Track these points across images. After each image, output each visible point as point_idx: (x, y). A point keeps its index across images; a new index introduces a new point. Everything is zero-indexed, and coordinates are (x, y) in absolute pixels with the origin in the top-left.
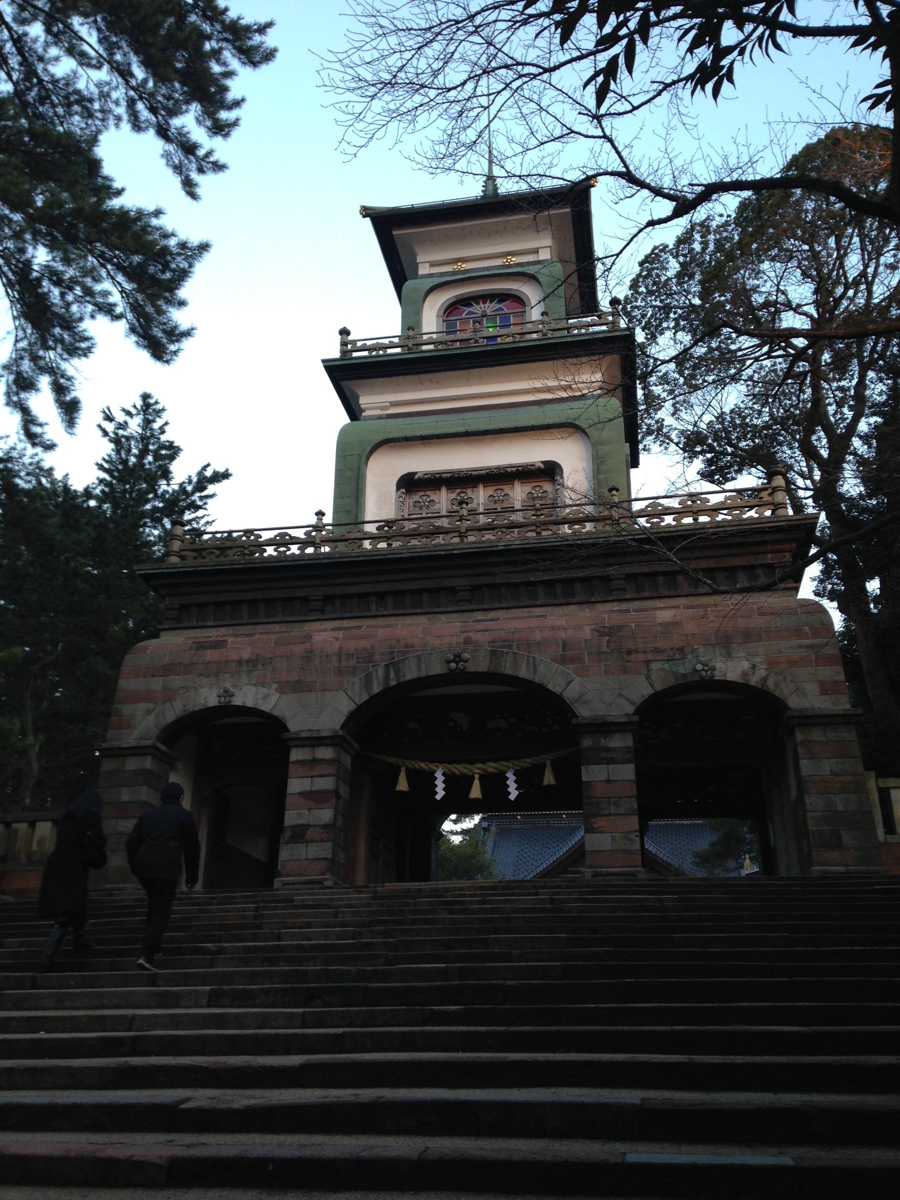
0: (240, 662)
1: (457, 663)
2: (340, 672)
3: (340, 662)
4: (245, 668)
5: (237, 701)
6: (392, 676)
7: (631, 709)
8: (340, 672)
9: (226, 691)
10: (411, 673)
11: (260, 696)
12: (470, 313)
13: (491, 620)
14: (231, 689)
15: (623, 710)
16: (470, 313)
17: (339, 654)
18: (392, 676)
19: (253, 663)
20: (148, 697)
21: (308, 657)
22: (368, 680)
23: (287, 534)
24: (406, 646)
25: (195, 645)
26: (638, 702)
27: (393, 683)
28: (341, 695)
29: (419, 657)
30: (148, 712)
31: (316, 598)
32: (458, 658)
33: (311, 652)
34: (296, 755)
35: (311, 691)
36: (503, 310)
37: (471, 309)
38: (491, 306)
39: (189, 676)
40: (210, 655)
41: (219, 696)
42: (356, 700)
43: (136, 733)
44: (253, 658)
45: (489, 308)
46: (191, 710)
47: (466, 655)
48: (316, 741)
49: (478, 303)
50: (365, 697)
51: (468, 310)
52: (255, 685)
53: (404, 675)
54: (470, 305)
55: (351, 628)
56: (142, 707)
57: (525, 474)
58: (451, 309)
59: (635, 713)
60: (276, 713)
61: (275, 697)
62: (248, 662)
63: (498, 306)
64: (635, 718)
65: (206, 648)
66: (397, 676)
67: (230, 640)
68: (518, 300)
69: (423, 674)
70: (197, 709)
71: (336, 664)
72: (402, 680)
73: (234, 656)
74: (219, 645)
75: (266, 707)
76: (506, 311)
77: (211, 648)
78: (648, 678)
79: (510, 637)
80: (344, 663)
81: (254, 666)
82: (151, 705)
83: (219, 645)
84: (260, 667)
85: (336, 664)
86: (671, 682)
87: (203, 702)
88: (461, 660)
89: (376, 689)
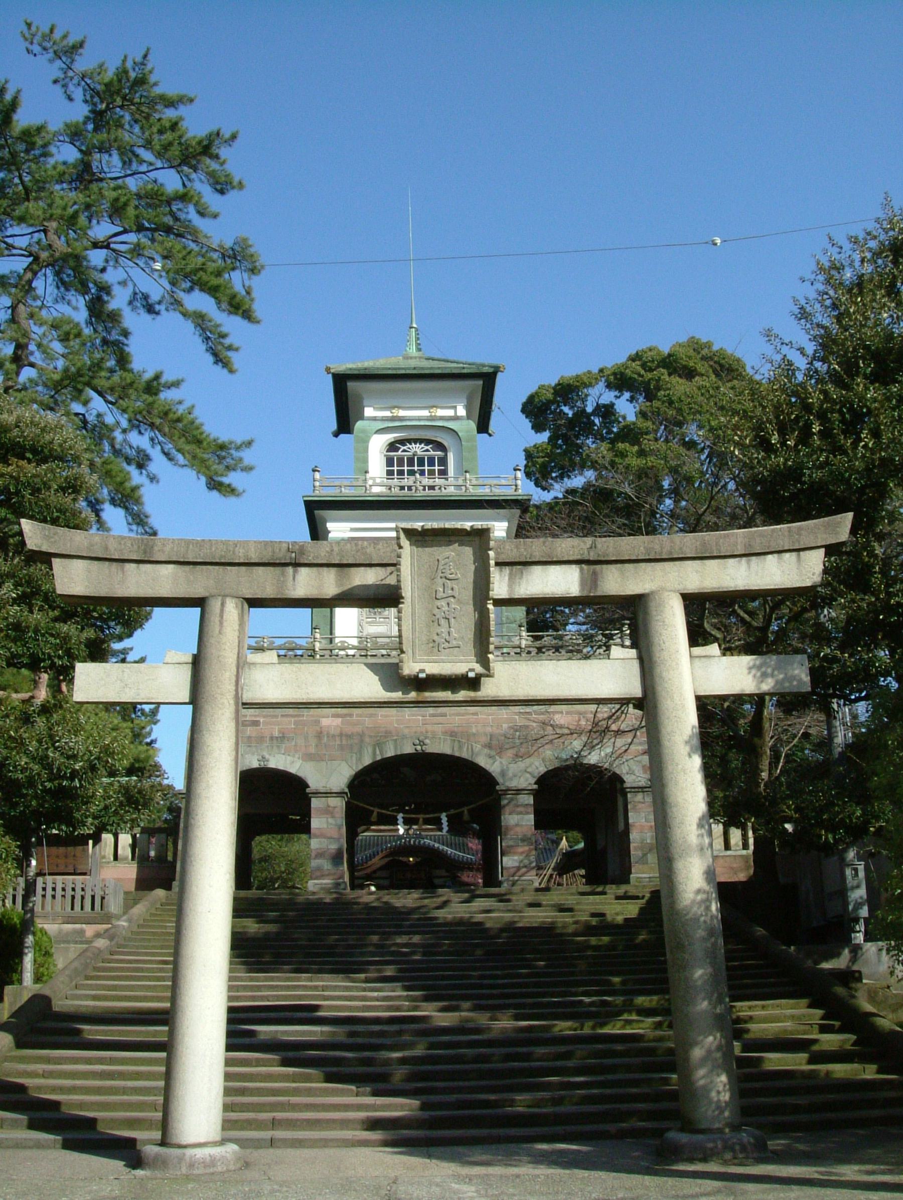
0: (272, 738)
2: (341, 748)
4: (275, 741)
6: (378, 752)
7: (533, 781)
8: (341, 748)
9: (263, 757)
10: (390, 753)
12: (404, 451)
14: (267, 756)
15: (527, 781)
16: (404, 451)
17: (341, 735)
18: (378, 752)
19: (282, 738)
21: (319, 735)
23: (293, 642)
24: (386, 732)
26: (537, 775)
27: (379, 758)
28: (344, 764)
29: (396, 740)
32: (422, 743)
33: (321, 732)
34: (315, 803)
37: (405, 448)
45: (418, 449)
47: (427, 741)
48: (328, 794)
49: (411, 444)
50: (360, 767)
51: (403, 448)
54: (404, 445)
55: (345, 715)
58: (392, 447)
59: (535, 783)
60: (300, 774)
63: (426, 448)
64: (535, 787)
66: (381, 753)
67: (261, 720)
69: (399, 753)
71: (338, 742)
74: (256, 723)
75: (293, 770)
76: (432, 453)
77: (250, 726)
78: (544, 760)
79: (456, 729)
80: (344, 742)
83: (256, 723)
85: (338, 742)
86: (557, 764)
88: (424, 744)
89: (367, 761)
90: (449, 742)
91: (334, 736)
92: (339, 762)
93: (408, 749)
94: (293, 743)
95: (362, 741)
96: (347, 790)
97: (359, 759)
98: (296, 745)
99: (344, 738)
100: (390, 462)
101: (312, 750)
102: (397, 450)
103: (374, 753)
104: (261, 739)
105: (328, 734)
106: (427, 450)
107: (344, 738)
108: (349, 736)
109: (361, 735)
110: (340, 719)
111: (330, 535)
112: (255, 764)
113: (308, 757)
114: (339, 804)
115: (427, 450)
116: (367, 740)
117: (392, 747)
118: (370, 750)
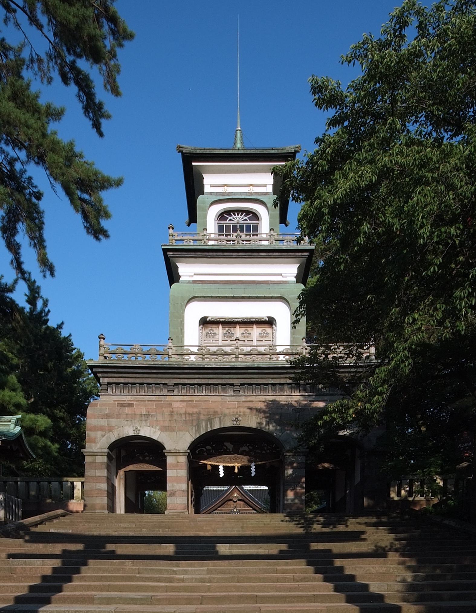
0: (141, 415)
1: (237, 422)
3: (186, 418)
4: (143, 417)
5: (142, 434)
6: (209, 426)
10: (217, 426)
11: (152, 432)
13: (250, 401)
18: (209, 426)
20: (101, 428)
22: (198, 426)
25: (119, 405)
27: (209, 430)
28: (187, 434)
30: (103, 436)
31: (171, 384)
32: (237, 420)
33: (173, 412)
35: (174, 431)
36: (247, 221)
37: (231, 218)
38: (241, 217)
39: (118, 420)
40: (127, 410)
41: (134, 431)
42: (194, 437)
43: (98, 446)
44: (147, 413)
46: (122, 437)
47: (240, 418)
50: (198, 436)
51: (230, 218)
52: (149, 426)
53: (214, 426)
54: (231, 216)
55: (189, 401)
56: (99, 433)
57: (259, 322)
58: (222, 216)
60: (159, 440)
61: (159, 433)
62: (145, 415)
63: (245, 218)
65: (125, 407)
66: (211, 427)
68: (255, 216)
69: (222, 427)
70: (124, 436)
72: (213, 429)
73: (138, 412)
75: (155, 438)
80: (187, 419)
81: (147, 417)
82: (104, 433)
84: (151, 418)
87: (126, 432)
90: (254, 418)
91: (181, 414)
92: (184, 432)
93: (228, 424)
94: (155, 419)
95: (198, 418)
96: (189, 451)
97: (198, 430)
98: (157, 421)
99: (187, 415)
100: (221, 228)
101: (167, 424)
102: (226, 219)
103: (206, 425)
104: (133, 416)
105: (177, 413)
106: (246, 220)
107: (187, 415)
108: (191, 415)
109: (199, 414)
110: (185, 403)
111: (181, 279)
112: (131, 433)
113: (164, 429)
114: (183, 460)
115: (246, 220)
116: (202, 417)
117: (218, 423)
118: (204, 424)
